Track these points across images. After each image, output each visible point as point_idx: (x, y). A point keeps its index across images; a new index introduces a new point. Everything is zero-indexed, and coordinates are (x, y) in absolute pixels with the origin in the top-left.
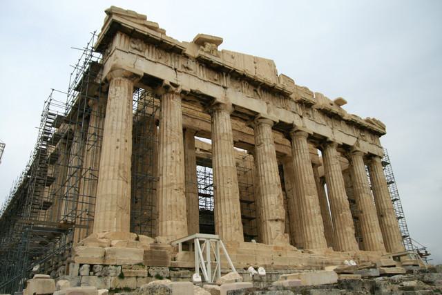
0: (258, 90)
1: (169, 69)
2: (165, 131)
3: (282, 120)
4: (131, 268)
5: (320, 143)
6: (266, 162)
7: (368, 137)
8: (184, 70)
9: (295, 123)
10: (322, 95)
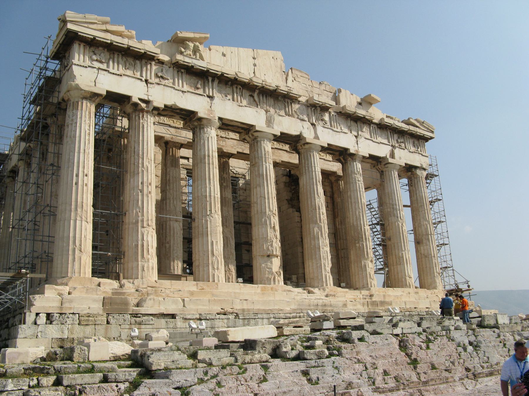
0: (255, 95)
1: (139, 81)
2: (132, 158)
3: (285, 131)
4: (89, 316)
5: (340, 155)
8: (157, 80)
9: (305, 135)
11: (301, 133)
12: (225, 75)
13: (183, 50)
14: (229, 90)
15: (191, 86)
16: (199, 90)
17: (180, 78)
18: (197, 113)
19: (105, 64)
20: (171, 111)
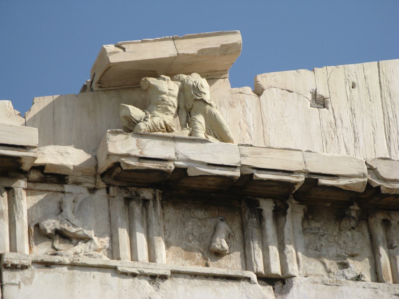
8: (42, 251)
12: (323, 181)
13: (136, 112)
14: (356, 239)
15: (188, 249)
16: (223, 261)
17: (138, 224)
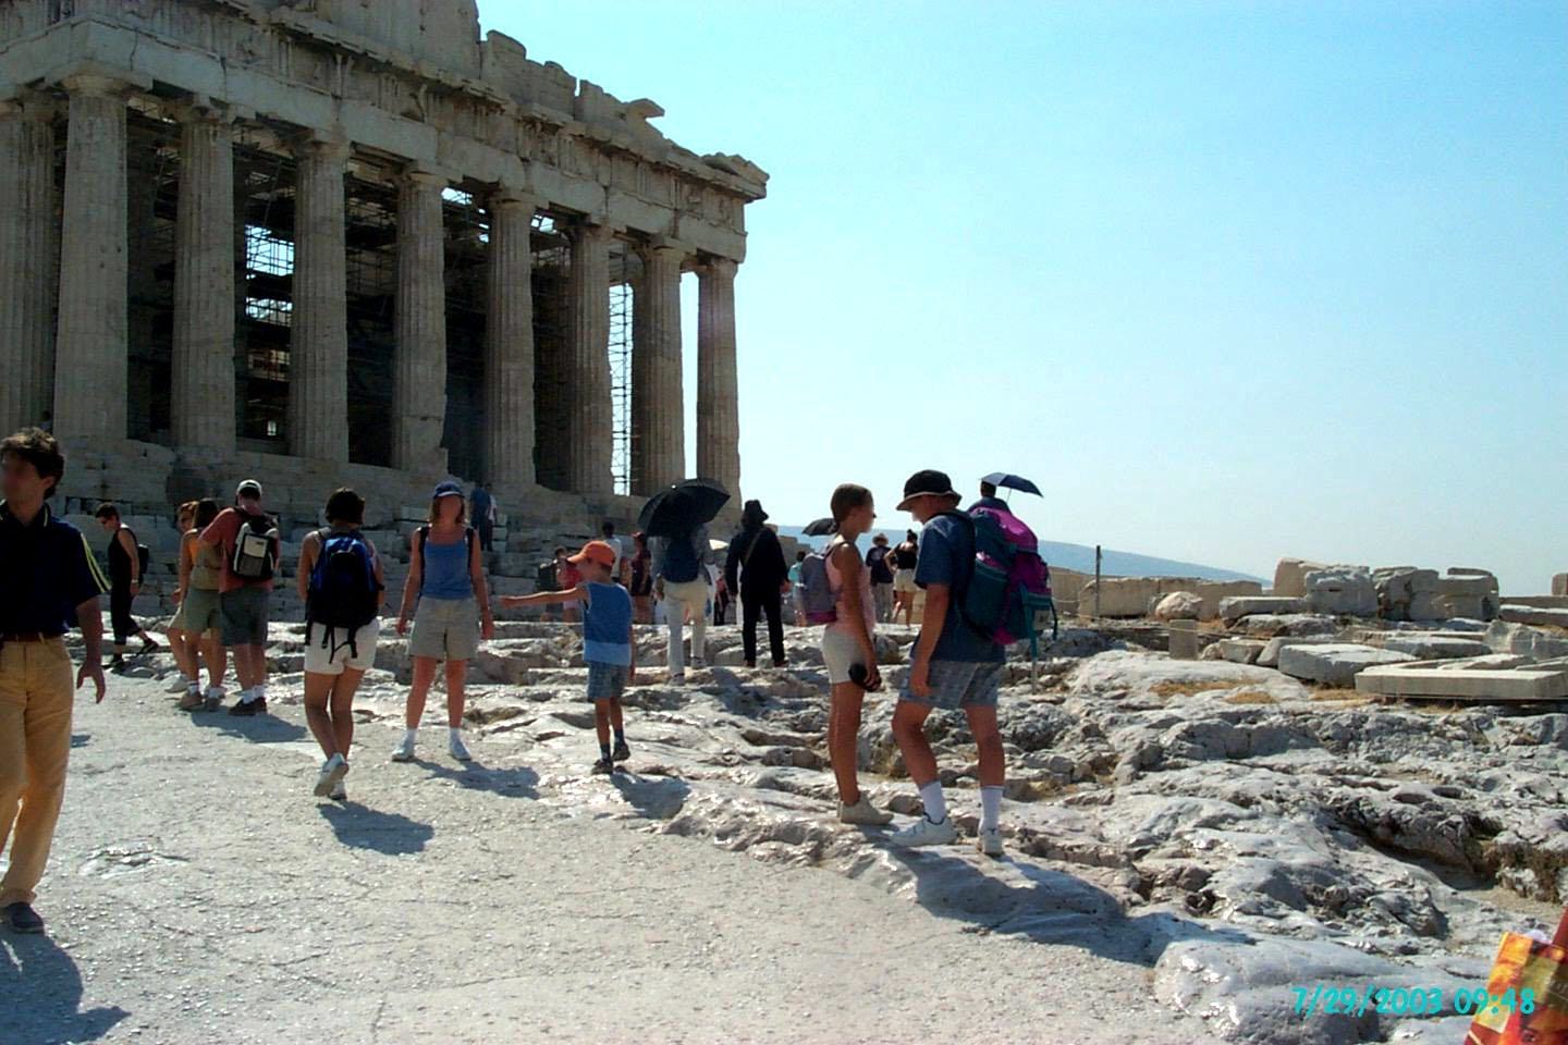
6: (417, 283)
7: (711, 204)
9: (508, 182)
10: (598, 88)
11: (500, 178)
12: (370, 55)
18: (313, 131)
19: (148, 20)
20: (265, 122)
